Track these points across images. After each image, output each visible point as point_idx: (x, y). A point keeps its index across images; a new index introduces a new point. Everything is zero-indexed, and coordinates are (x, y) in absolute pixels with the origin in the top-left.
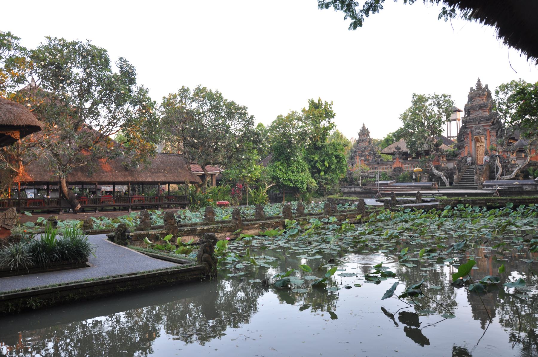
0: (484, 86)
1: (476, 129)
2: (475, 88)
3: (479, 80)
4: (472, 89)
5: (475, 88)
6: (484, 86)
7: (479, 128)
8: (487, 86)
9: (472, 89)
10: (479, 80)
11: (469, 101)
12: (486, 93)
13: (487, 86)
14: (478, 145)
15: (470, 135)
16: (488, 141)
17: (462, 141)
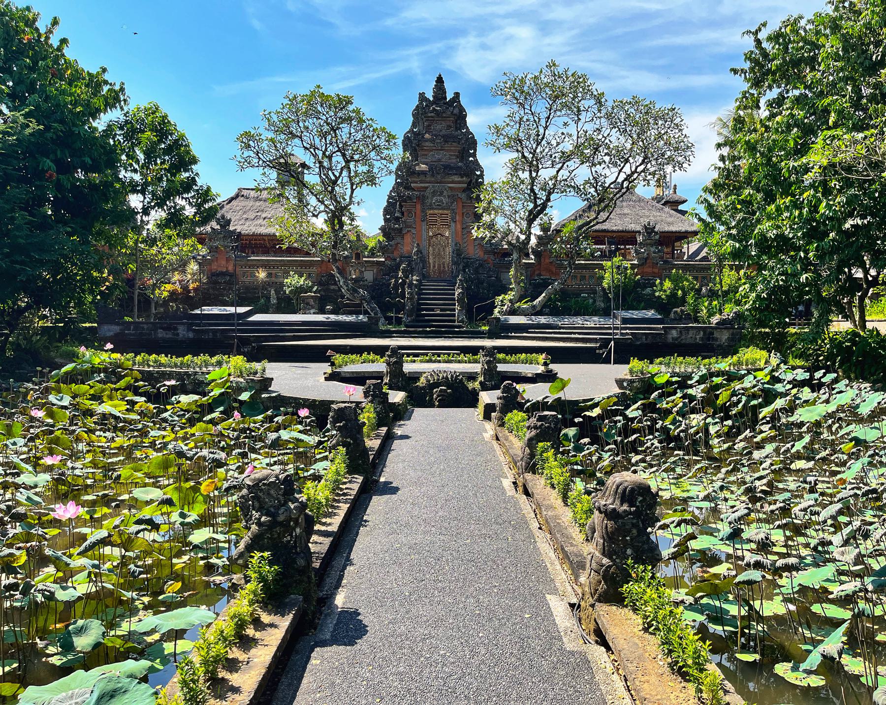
0: (449, 96)
1: (434, 193)
2: (430, 96)
3: (440, 80)
4: (422, 96)
5: (430, 96)
6: (449, 96)
7: (441, 194)
8: (457, 95)
9: (422, 96)
10: (440, 80)
11: (414, 125)
12: (456, 111)
13: (457, 95)
14: (431, 234)
15: (419, 207)
16: (459, 226)
17: (397, 219)
